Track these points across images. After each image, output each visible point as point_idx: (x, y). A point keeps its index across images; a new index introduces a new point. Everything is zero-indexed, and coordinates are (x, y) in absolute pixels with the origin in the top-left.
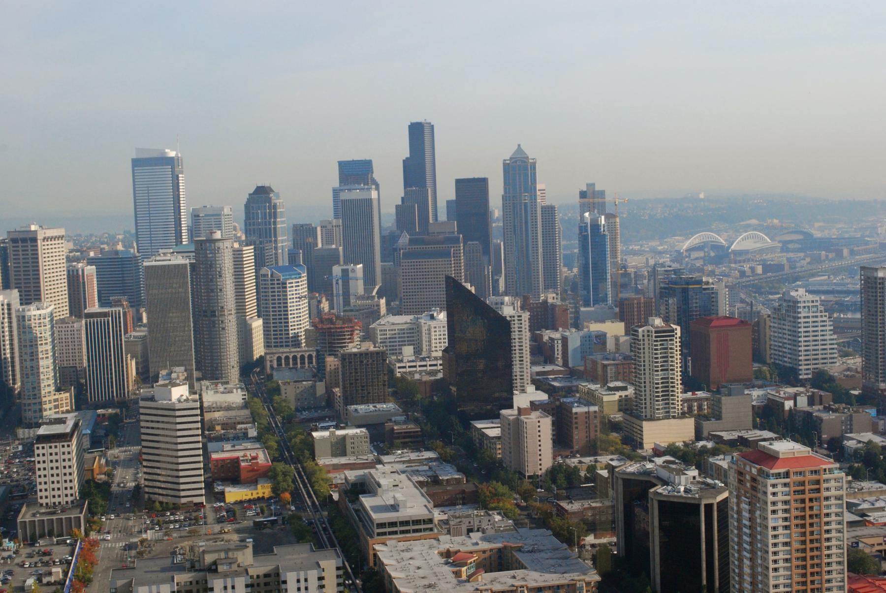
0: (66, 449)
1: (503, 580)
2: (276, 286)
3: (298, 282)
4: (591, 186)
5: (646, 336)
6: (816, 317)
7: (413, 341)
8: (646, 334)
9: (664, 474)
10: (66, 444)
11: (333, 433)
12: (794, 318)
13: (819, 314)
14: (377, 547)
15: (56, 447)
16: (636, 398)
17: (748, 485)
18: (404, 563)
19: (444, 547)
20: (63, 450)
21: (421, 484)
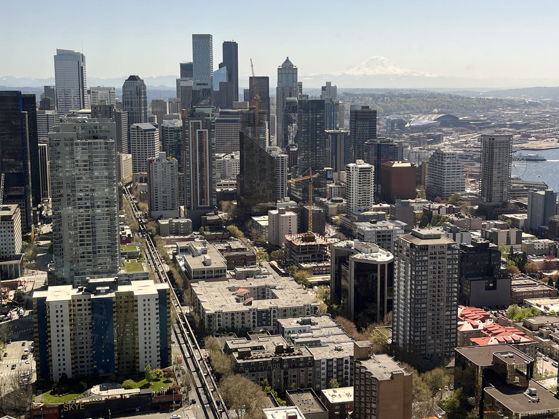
0: (10, 225)
1: (262, 304)
2: (140, 135)
3: (154, 134)
4: (329, 84)
5: (354, 170)
6: (455, 163)
7: (221, 170)
8: (354, 169)
9: (359, 248)
10: (10, 222)
11: (171, 222)
12: (442, 163)
13: (456, 162)
14: (192, 284)
15: (4, 224)
16: (347, 206)
17: (405, 253)
18: (207, 294)
19: (231, 285)
20: (8, 225)
21: (221, 251)
